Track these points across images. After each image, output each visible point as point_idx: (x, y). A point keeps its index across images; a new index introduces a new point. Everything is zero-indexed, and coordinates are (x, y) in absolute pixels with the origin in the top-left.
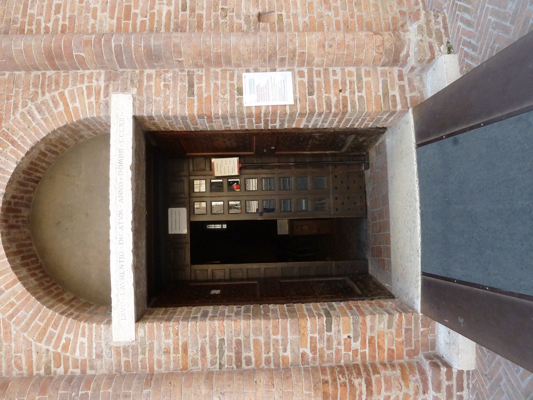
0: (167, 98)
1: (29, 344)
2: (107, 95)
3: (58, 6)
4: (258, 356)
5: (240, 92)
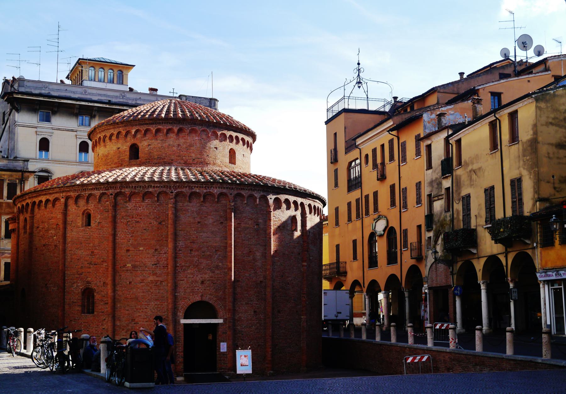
1: (181, 305)
2: (223, 318)
4: (177, 345)
5: (223, 342)
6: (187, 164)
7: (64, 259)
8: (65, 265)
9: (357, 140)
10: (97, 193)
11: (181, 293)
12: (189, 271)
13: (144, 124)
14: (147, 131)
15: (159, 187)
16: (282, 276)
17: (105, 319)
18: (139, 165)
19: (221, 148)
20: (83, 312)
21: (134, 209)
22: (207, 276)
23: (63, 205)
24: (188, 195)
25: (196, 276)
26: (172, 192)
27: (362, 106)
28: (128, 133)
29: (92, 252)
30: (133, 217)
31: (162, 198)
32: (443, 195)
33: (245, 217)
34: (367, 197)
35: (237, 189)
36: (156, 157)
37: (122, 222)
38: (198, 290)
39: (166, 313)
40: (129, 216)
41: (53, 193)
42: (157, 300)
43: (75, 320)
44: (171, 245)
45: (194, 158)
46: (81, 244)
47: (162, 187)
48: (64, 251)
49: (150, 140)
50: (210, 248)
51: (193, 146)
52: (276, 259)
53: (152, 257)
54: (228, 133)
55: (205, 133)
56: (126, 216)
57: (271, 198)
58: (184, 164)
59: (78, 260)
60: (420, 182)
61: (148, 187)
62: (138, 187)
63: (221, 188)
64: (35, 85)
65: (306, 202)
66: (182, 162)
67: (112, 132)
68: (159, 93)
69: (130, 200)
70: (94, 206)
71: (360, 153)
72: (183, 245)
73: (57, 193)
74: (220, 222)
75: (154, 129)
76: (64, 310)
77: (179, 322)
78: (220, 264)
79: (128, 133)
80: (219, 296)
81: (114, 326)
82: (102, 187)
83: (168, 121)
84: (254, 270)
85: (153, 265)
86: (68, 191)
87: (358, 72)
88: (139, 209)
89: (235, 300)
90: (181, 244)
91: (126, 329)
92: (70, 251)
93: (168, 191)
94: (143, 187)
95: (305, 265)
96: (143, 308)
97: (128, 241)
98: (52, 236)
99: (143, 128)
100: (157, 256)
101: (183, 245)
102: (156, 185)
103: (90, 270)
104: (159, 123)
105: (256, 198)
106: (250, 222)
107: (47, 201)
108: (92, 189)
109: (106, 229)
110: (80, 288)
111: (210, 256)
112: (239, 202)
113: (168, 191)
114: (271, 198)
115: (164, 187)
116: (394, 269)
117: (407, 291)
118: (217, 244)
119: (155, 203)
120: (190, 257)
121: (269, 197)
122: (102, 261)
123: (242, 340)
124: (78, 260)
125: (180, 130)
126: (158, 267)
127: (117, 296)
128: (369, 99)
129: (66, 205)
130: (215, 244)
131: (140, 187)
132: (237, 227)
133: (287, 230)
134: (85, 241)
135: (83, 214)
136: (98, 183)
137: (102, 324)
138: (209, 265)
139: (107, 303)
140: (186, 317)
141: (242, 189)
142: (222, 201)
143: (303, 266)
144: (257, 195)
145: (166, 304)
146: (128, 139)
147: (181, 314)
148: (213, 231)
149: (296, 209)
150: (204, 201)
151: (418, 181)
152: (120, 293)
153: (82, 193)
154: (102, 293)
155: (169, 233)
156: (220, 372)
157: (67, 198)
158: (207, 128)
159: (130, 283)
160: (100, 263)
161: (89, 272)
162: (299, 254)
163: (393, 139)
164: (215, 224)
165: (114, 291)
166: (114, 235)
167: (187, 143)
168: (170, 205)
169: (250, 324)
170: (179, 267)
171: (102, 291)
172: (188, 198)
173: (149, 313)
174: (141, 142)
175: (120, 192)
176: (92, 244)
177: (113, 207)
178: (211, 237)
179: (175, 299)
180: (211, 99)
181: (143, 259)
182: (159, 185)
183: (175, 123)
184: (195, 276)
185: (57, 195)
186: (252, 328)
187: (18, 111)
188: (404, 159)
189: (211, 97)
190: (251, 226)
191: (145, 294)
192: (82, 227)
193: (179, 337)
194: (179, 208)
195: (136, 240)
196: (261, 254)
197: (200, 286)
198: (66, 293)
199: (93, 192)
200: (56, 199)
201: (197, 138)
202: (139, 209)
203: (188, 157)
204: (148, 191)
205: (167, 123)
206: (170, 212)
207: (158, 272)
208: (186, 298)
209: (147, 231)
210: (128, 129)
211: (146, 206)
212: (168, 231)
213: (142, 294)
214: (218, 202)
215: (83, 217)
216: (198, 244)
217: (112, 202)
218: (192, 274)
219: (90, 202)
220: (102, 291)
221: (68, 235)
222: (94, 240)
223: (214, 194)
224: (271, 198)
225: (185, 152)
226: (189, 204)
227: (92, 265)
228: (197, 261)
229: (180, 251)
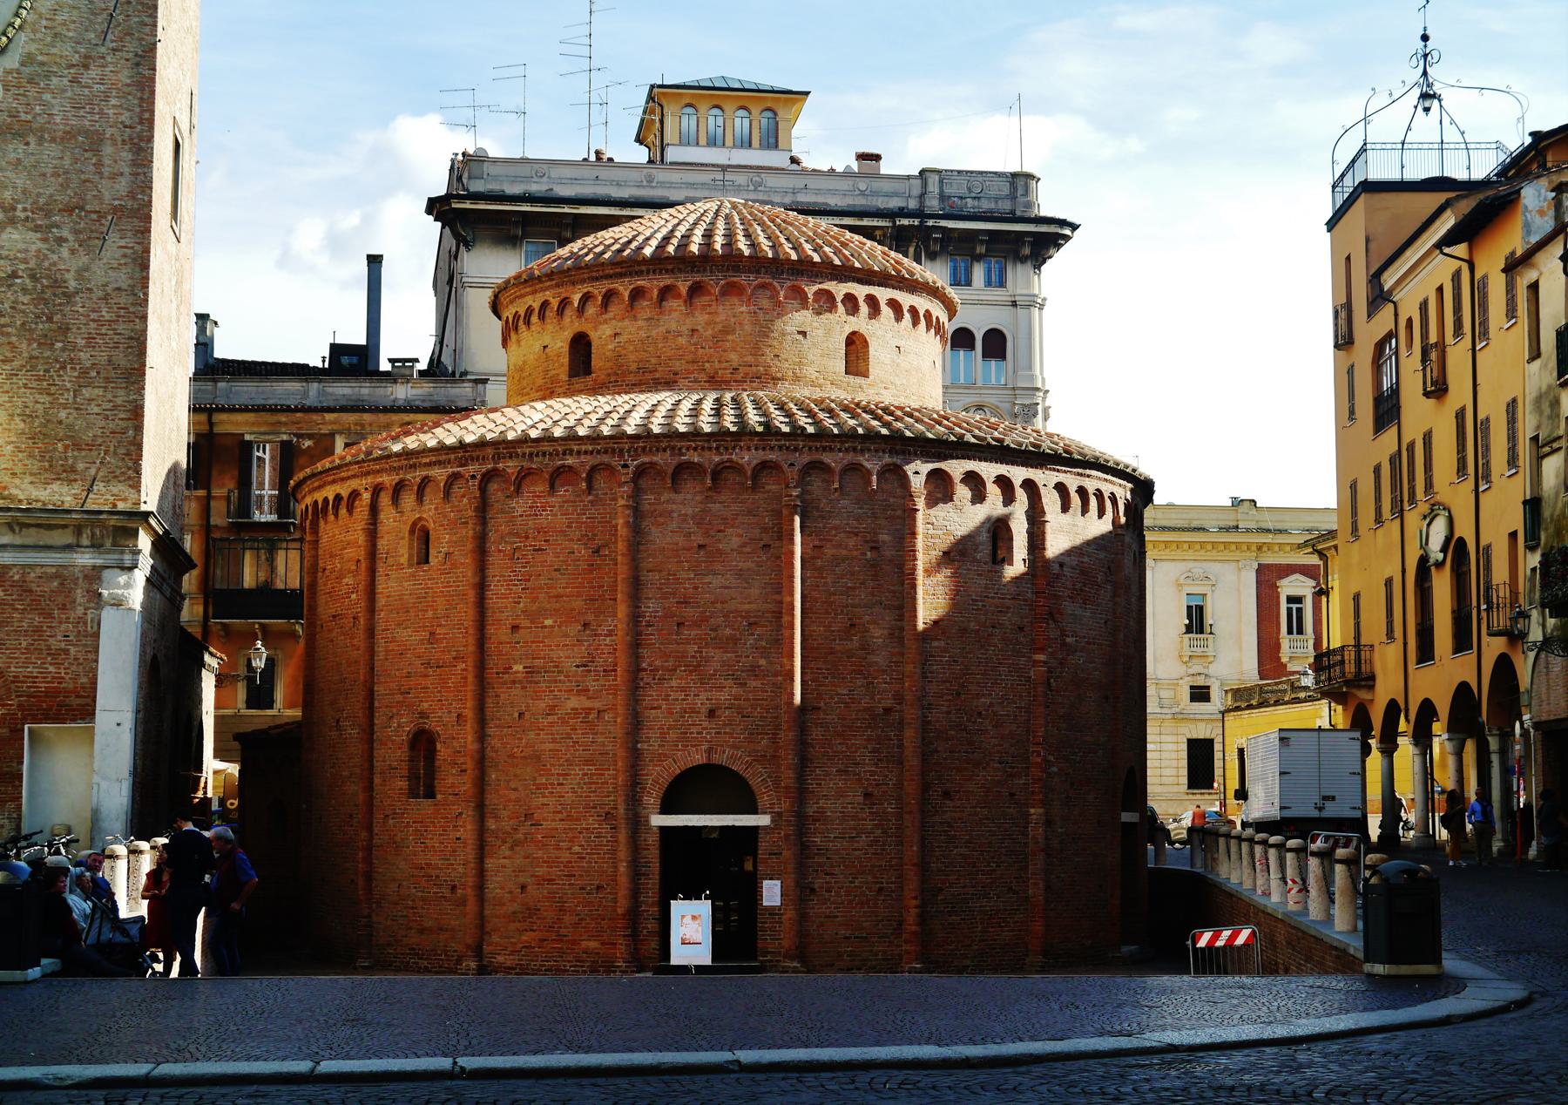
0: (768, 842)
3: (820, 784)
4: (641, 884)
6: (717, 381)
7: (371, 652)
8: (372, 669)
9: (1385, 276)
10: (440, 474)
11: (651, 743)
12: (674, 683)
13: (601, 277)
14: (609, 296)
15: (592, 452)
16: (959, 694)
17: (461, 814)
18: (595, 390)
19: (820, 332)
20: (413, 793)
21: (530, 515)
22: (723, 696)
23: (367, 508)
24: (670, 471)
25: (695, 695)
26: (625, 466)
27: (1419, 170)
28: (564, 303)
29: (433, 634)
30: (527, 537)
31: (601, 482)
32: (1560, 437)
33: (836, 528)
34: (1411, 446)
35: (810, 448)
36: (633, 367)
37: (500, 551)
38: (698, 733)
40: (517, 535)
41: (349, 478)
42: (588, 762)
43: (395, 813)
44: (622, 610)
45: (735, 365)
46: (408, 612)
47: (599, 452)
48: (371, 632)
49: (619, 320)
50: (734, 617)
51: (733, 332)
52: (935, 644)
53: (575, 645)
54: (840, 289)
55: (768, 293)
56: (510, 534)
57: (917, 473)
58: (709, 382)
59: (402, 654)
60: (1514, 401)
61: (564, 454)
62: (537, 455)
63: (764, 449)
64: (512, 170)
65: (1046, 478)
66: (702, 377)
67: (530, 303)
68: (886, 168)
69: (518, 491)
70: (436, 509)
71: (1396, 315)
72: (657, 612)
73: (354, 476)
74: (762, 543)
75: (626, 290)
76: (370, 788)
77: (648, 821)
78: (763, 662)
79: (564, 303)
80: (758, 751)
81: (481, 831)
82: (453, 456)
84: (865, 678)
85: (577, 666)
86: (378, 471)
87: (1422, 62)
88: (541, 515)
89: (803, 762)
90: (651, 607)
91: (511, 841)
92: (383, 630)
93: (615, 462)
94: (551, 454)
95: (1040, 661)
96: (553, 784)
97: (515, 602)
98: (348, 593)
99: (599, 289)
100: (586, 641)
101: (657, 612)
102: (584, 448)
103: (428, 682)
104: (639, 273)
105: (869, 473)
106: (851, 543)
107: (338, 498)
108: (430, 464)
109: (462, 572)
110: (404, 731)
111: (734, 640)
112: (816, 484)
113: (615, 462)
114: (917, 473)
115: (606, 452)
117: (1495, 732)
118: (753, 606)
119: (583, 497)
120: (678, 644)
121: (910, 469)
122: (454, 658)
123: (826, 874)
124: (402, 654)
125: (696, 290)
126: (590, 671)
127: (488, 751)
128: (1445, 146)
129: (374, 509)
130: (747, 607)
131: (544, 454)
132: (813, 558)
133: (975, 560)
134: (415, 603)
135: (412, 532)
136: (442, 448)
137: (454, 826)
138: (729, 666)
139: (465, 771)
140: (665, 810)
141: (824, 449)
142: (769, 484)
143: (1036, 663)
144: (872, 464)
145: (611, 772)
146: (567, 319)
147: (652, 799)
148: (741, 570)
149: (1009, 498)
150: (715, 488)
151: (1509, 399)
152: (496, 742)
153: (408, 477)
154: (455, 744)
155: (619, 578)
156: (762, 962)
157: (377, 490)
158: (774, 278)
159: (520, 715)
162: (1021, 629)
163: (1460, 267)
164: (748, 549)
165: (482, 737)
166: (481, 587)
167: (715, 323)
168: (621, 502)
169: (850, 829)
170: (646, 670)
171: (454, 738)
172: (669, 481)
173: (569, 798)
174: (596, 329)
175: (495, 469)
176: (430, 614)
177: (476, 509)
178: (735, 587)
179: (635, 759)
180: (1014, 175)
181: (552, 650)
182: (590, 448)
183: (680, 271)
184: (689, 695)
185: (354, 484)
186: (858, 842)
187: (468, 246)
188: (1481, 331)
189: (1015, 168)
190: (855, 553)
191: (557, 746)
192: (410, 565)
193: (646, 862)
194: (646, 507)
195: (534, 599)
196: (886, 632)
197: (705, 724)
198: (375, 745)
200: (355, 495)
201: (744, 309)
202: (541, 515)
203: (719, 362)
204: (563, 466)
205: (661, 270)
206: (621, 521)
207: (592, 685)
208: (665, 755)
209: (561, 574)
210: (563, 292)
211: (560, 506)
212: (616, 574)
213: (551, 746)
214: (754, 488)
215: (411, 540)
216: (699, 607)
217: (475, 498)
218: (682, 689)
219: (426, 498)
220: (454, 738)
221: (379, 588)
222: (436, 601)
223: (742, 466)
224: (918, 472)
225: (710, 348)
226: (673, 496)
227: (431, 667)
228: (698, 655)
229: (651, 626)
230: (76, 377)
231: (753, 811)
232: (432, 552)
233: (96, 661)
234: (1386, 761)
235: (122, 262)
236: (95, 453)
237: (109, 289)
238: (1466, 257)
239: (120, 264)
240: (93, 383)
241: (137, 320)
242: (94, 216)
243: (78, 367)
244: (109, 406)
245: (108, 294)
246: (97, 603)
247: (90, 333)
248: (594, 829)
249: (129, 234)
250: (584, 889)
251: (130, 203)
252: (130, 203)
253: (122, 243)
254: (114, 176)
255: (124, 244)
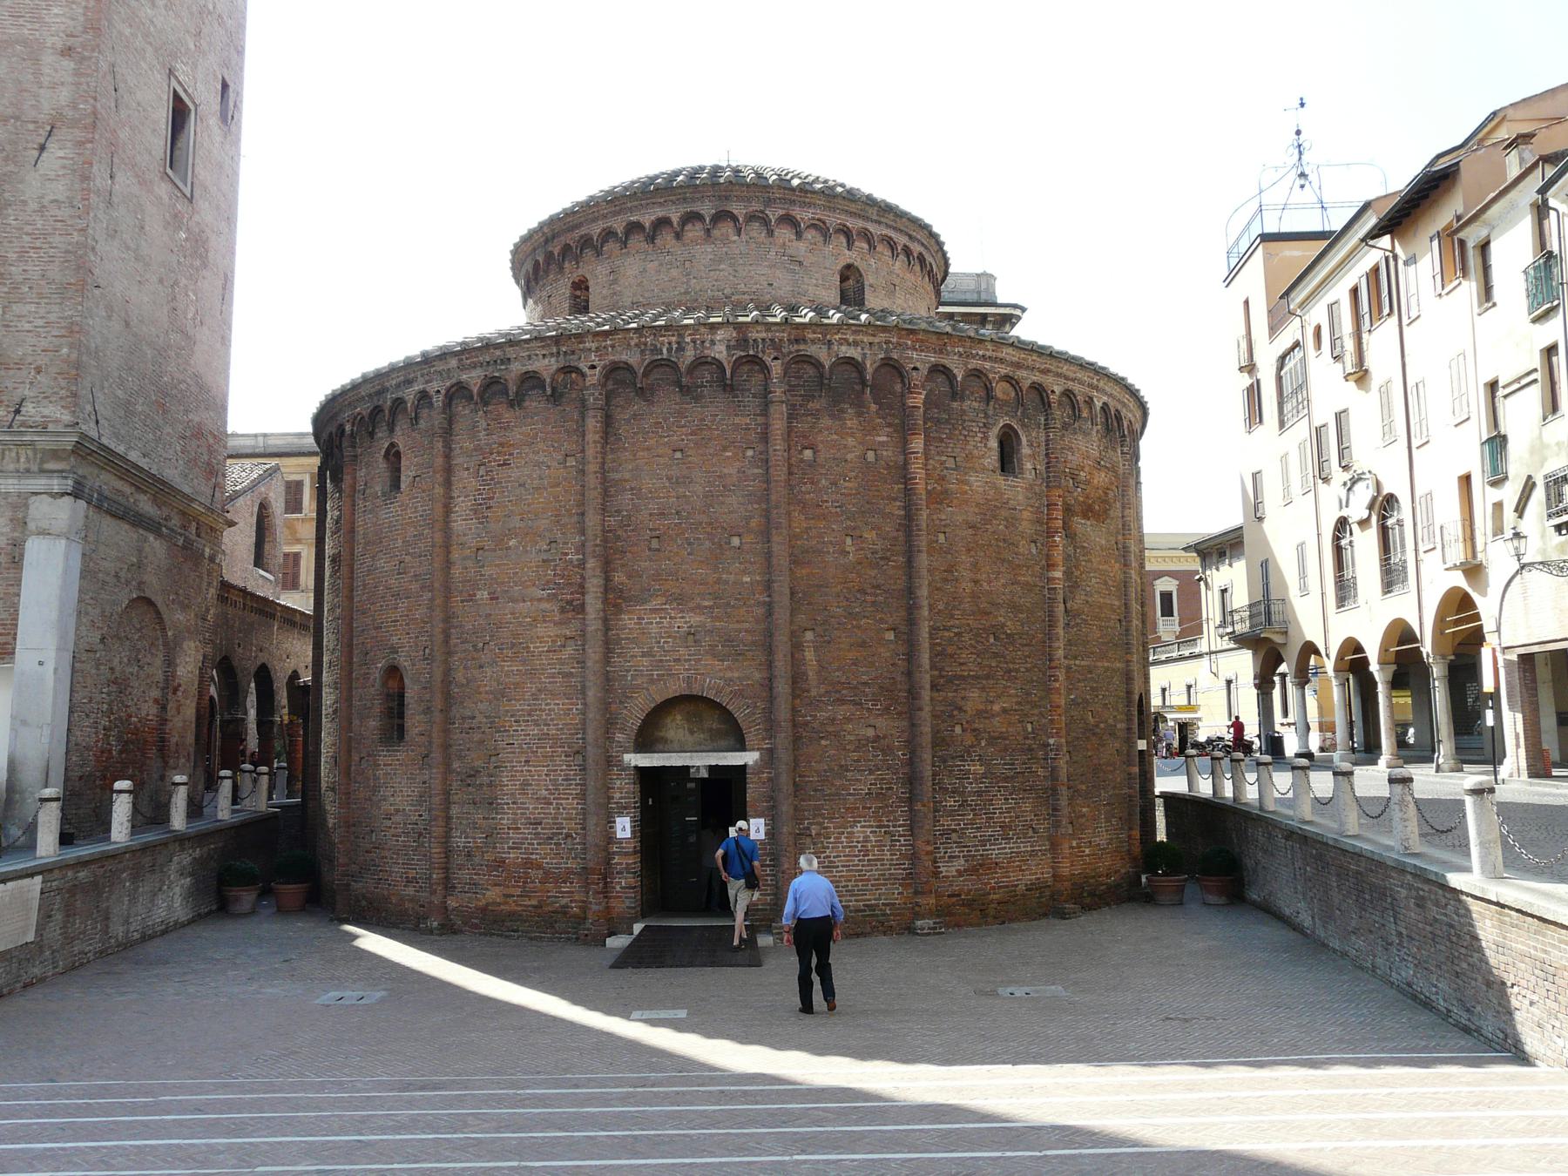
2: (758, 749)
32: (1536, 370)
39: (580, 736)
57: (915, 369)
83: (654, 200)
95: (1054, 579)
114: (915, 369)
116: (1402, 606)
160: (418, 593)
161: (395, 621)
166: (448, 510)
199: (400, 394)
230: (6, 293)
231: (742, 747)
232: (403, 478)
233: (19, 595)
234: (1300, 692)
235: (60, 173)
236: (24, 373)
237: (45, 202)
238: (1390, 248)
239: (59, 176)
240: (25, 298)
241: (75, 233)
242: (31, 127)
243: (8, 282)
244: (40, 322)
245: (44, 207)
246: (23, 532)
247: (23, 247)
248: (561, 770)
249: (69, 145)
250: (551, 839)
251: (71, 113)
252: (71, 113)
253: (61, 153)
254: (53, 85)
255: (62, 155)
